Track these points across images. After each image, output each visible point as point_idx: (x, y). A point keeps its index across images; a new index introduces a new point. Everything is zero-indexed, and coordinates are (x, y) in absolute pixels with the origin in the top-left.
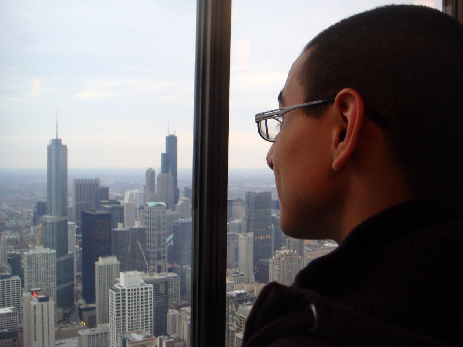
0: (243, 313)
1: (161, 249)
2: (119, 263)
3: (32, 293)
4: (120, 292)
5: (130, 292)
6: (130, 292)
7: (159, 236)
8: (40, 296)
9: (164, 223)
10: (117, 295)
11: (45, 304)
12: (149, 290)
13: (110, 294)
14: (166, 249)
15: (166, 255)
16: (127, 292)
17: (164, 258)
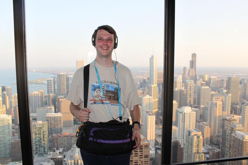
0: (233, 126)
1: (191, 99)
2: (177, 103)
3: (147, 112)
4: (183, 114)
5: (187, 114)
6: (187, 114)
7: (190, 93)
8: (150, 114)
9: (192, 89)
10: (182, 115)
11: (152, 116)
12: (194, 114)
13: (179, 114)
14: (193, 99)
15: (193, 101)
16: (186, 114)
17: (192, 102)
